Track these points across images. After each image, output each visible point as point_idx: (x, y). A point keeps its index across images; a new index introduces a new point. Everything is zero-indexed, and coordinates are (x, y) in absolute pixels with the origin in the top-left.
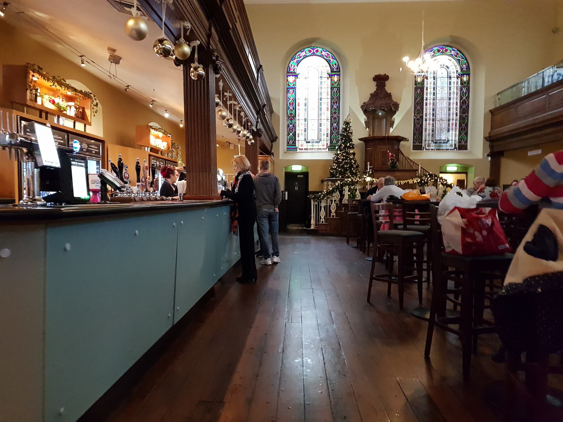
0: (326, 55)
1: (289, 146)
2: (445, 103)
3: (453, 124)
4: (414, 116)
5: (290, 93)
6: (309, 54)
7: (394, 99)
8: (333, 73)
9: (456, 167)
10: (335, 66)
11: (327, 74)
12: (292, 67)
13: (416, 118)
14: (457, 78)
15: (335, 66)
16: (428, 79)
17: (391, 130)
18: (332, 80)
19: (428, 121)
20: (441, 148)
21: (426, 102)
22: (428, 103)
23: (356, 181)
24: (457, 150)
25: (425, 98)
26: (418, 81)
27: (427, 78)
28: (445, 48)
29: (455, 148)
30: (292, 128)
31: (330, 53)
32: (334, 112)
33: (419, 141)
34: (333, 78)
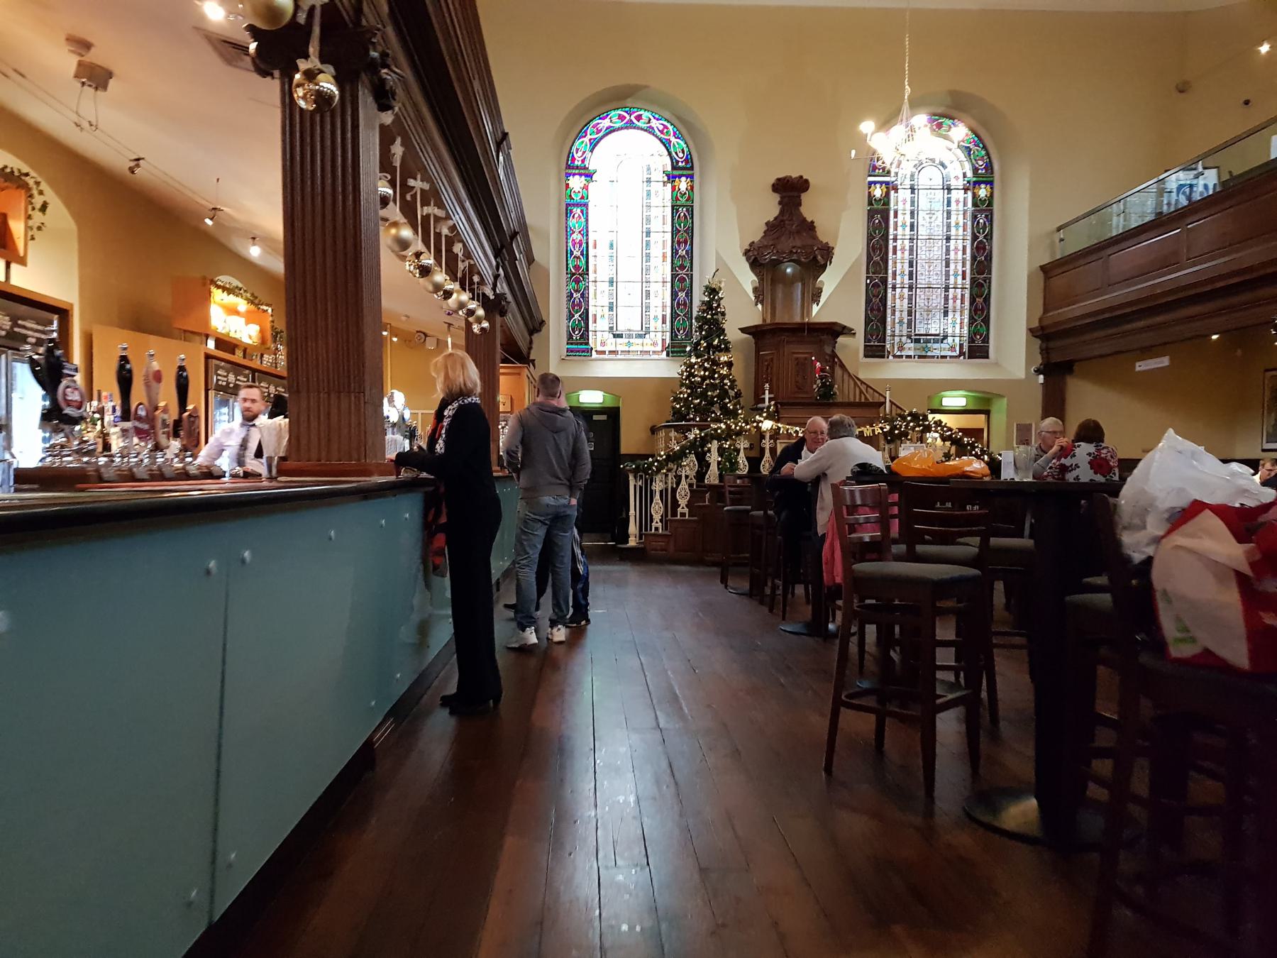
0: (661, 127)
1: (572, 344)
2: (938, 247)
3: (955, 298)
4: (867, 278)
5: (573, 217)
6: (619, 124)
7: (823, 235)
8: (676, 173)
9: (965, 399)
13: (871, 282)
14: (966, 190)
17: (815, 309)
18: (673, 189)
19: (898, 291)
20: (929, 354)
21: (895, 244)
22: (899, 248)
23: (738, 428)
24: (964, 358)
25: (891, 237)
26: (874, 196)
27: (896, 190)
29: (962, 353)
30: (580, 301)
31: (668, 125)
32: (678, 265)
33: (878, 336)
34: (676, 184)
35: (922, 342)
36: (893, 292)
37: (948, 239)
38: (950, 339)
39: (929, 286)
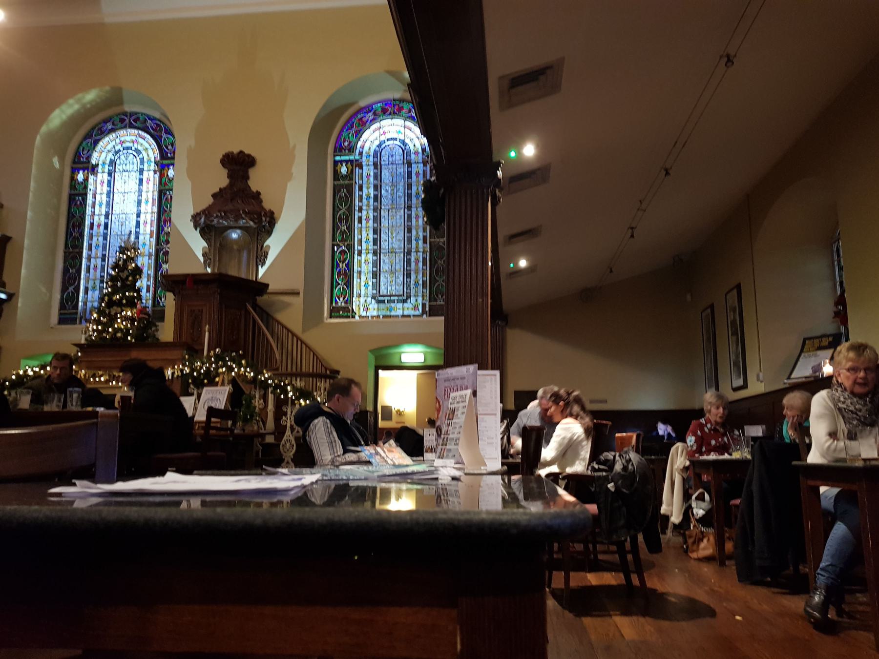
0: (154, 126)
2: (401, 216)
3: (417, 261)
4: (333, 246)
6: (120, 125)
7: (267, 205)
8: (165, 162)
10: (170, 147)
11: (155, 163)
12: (85, 152)
14: (425, 164)
15: (170, 147)
16: (362, 169)
17: (262, 271)
18: (161, 176)
19: (363, 256)
20: (393, 313)
21: (360, 214)
22: (364, 217)
24: (427, 316)
25: (357, 208)
26: (341, 173)
27: (361, 166)
29: (424, 311)
33: (344, 298)
37: (409, 208)
38: (413, 299)
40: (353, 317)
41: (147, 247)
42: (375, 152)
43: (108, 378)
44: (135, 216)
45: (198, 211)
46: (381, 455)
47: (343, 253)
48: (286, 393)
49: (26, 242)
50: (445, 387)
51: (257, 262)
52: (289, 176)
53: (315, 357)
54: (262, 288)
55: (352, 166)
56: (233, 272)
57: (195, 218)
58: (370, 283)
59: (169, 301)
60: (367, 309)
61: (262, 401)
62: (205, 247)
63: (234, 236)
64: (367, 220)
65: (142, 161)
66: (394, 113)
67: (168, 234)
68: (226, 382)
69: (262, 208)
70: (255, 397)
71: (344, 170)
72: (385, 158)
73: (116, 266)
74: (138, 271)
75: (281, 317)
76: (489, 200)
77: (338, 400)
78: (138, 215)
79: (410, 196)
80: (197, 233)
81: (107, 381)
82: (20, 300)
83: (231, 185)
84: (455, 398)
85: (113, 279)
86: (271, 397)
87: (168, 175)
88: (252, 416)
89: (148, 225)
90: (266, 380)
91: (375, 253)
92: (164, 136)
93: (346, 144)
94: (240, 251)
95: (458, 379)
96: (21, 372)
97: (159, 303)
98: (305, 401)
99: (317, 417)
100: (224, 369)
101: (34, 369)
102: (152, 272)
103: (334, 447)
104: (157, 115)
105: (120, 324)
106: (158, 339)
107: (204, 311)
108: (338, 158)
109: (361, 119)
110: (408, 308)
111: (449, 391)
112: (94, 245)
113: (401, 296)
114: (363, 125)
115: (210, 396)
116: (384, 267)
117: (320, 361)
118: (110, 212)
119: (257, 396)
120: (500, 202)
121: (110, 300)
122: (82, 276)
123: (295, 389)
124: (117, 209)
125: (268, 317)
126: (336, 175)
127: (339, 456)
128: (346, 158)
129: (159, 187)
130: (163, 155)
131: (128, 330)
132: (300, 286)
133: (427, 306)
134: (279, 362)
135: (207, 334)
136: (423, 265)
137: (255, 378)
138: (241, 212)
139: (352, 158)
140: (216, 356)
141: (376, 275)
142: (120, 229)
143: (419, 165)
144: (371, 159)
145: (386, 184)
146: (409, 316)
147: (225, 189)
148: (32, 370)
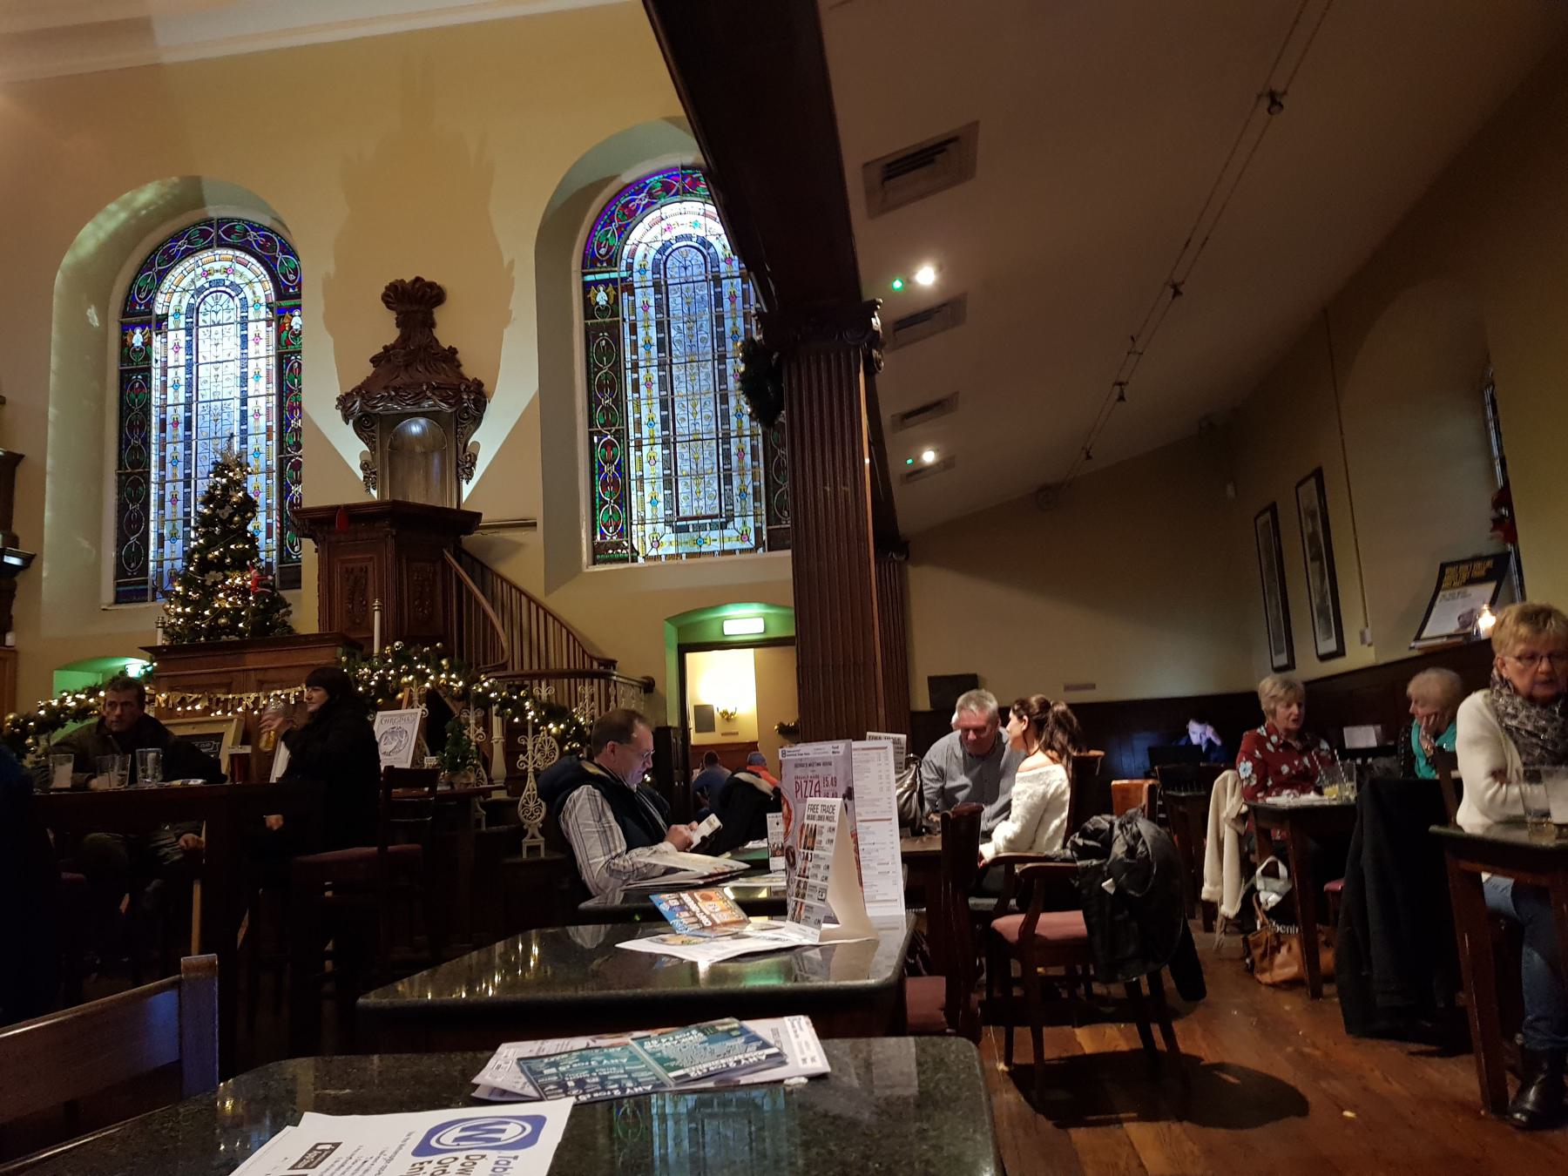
0: (262, 240)
1: (126, 584)
2: (707, 374)
3: (741, 453)
4: (591, 435)
7: (470, 371)
9: (762, 620)
10: (292, 277)
11: (267, 307)
12: (142, 296)
13: (599, 440)
15: (292, 277)
16: (633, 294)
17: (467, 489)
18: (280, 329)
19: (646, 449)
21: (635, 376)
22: (642, 381)
24: (764, 551)
26: (597, 303)
27: (631, 290)
28: (691, 175)
29: (759, 543)
32: (291, 442)
34: (286, 321)
35: (691, 530)
36: (638, 453)
37: (722, 359)
39: (696, 437)
40: (634, 560)
41: (263, 457)
42: (656, 263)
43: (207, 704)
44: (237, 403)
45: (349, 390)
46: (689, 910)
47: (609, 448)
48: (523, 713)
49: (49, 462)
50: (797, 777)
51: (457, 472)
52: (506, 319)
53: (571, 637)
54: (470, 520)
55: (616, 289)
56: (417, 496)
57: (344, 402)
58: (661, 498)
59: (308, 553)
60: (657, 543)
61: (481, 730)
62: (364, 452)
63: (415, 429)
64: (649, 385)
65: (244, 305)
66: (685, 192)
67: (298, 431)
68: (416, 698)
69: (462, 377)
70: (469, 725)
71: (601, 298)
72: (674, 273)
73: (209, 498)
74: (249, 506)
75: (507, 569)
76: (859, 372)
77: (613, 751)
78: (244, 402)
79: (721, 337)
80: (350, 428)
81: (207, 711)
82: (45, 565)
83: (403, 340)
84: (814, 808)
85: (205, 521)
86: (496, 722)
87: (291, 327)
88: (464, 759)
89: (263, 419)
90: (487, 691)
91: (665, 443)
92: (280, 257)
93: (603, 251)
94: (426, 454)
95: (819, 764)
96: (55, 703)
97: (289, 555)
98: (557, 725)
99: (577, 787)
100: (411, 678)
101: (78, 696)
102: (274, 501)
103: (610, 839)
104: (266, 221)
105: (223, 601)
106: (290, 630)
107: (370, 569)
108: (589, 278)
109: (625, 206)
110: (731, 538)
111: (804, 784)
112: (168, 459)
113: (716, 517)
114: (631, 216)
115: (388, 727)
116: (684, 467)
117: (579, 645)
118: (194, 398)
119: (472, 721)
120: (880, 369)
121: (203, 559)
122: (152, 517)
123: (538, 705)
124: (205, 392)
125: (482, 570)
126: (589, 309)
127: (619, 855)
128: (606, 276)
129: (277, 349)
130: (281, 291)
131: (238, 610)
132: (536, 512)
133: (764, 532)
134: (507, 654)
135: (377, 615)
136: (753, 459)
137: (466, 689)
138: (425, 387)
139: (613, 275)
140: (395, 654)
141: (670, 482)
142: (213, 427)
143: (735, 281)
144: (649, 275)
145: (678, 318)
146: (732, 552)
147: (393, 347)
148: (74, 699)
